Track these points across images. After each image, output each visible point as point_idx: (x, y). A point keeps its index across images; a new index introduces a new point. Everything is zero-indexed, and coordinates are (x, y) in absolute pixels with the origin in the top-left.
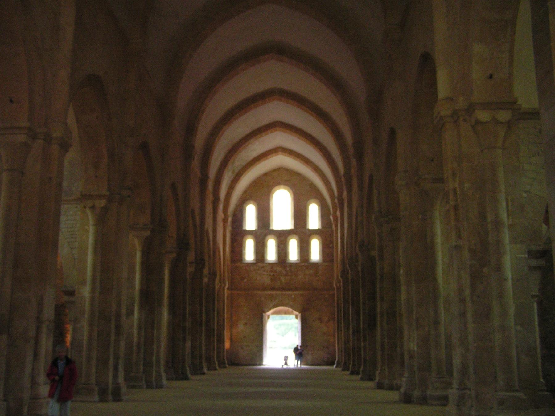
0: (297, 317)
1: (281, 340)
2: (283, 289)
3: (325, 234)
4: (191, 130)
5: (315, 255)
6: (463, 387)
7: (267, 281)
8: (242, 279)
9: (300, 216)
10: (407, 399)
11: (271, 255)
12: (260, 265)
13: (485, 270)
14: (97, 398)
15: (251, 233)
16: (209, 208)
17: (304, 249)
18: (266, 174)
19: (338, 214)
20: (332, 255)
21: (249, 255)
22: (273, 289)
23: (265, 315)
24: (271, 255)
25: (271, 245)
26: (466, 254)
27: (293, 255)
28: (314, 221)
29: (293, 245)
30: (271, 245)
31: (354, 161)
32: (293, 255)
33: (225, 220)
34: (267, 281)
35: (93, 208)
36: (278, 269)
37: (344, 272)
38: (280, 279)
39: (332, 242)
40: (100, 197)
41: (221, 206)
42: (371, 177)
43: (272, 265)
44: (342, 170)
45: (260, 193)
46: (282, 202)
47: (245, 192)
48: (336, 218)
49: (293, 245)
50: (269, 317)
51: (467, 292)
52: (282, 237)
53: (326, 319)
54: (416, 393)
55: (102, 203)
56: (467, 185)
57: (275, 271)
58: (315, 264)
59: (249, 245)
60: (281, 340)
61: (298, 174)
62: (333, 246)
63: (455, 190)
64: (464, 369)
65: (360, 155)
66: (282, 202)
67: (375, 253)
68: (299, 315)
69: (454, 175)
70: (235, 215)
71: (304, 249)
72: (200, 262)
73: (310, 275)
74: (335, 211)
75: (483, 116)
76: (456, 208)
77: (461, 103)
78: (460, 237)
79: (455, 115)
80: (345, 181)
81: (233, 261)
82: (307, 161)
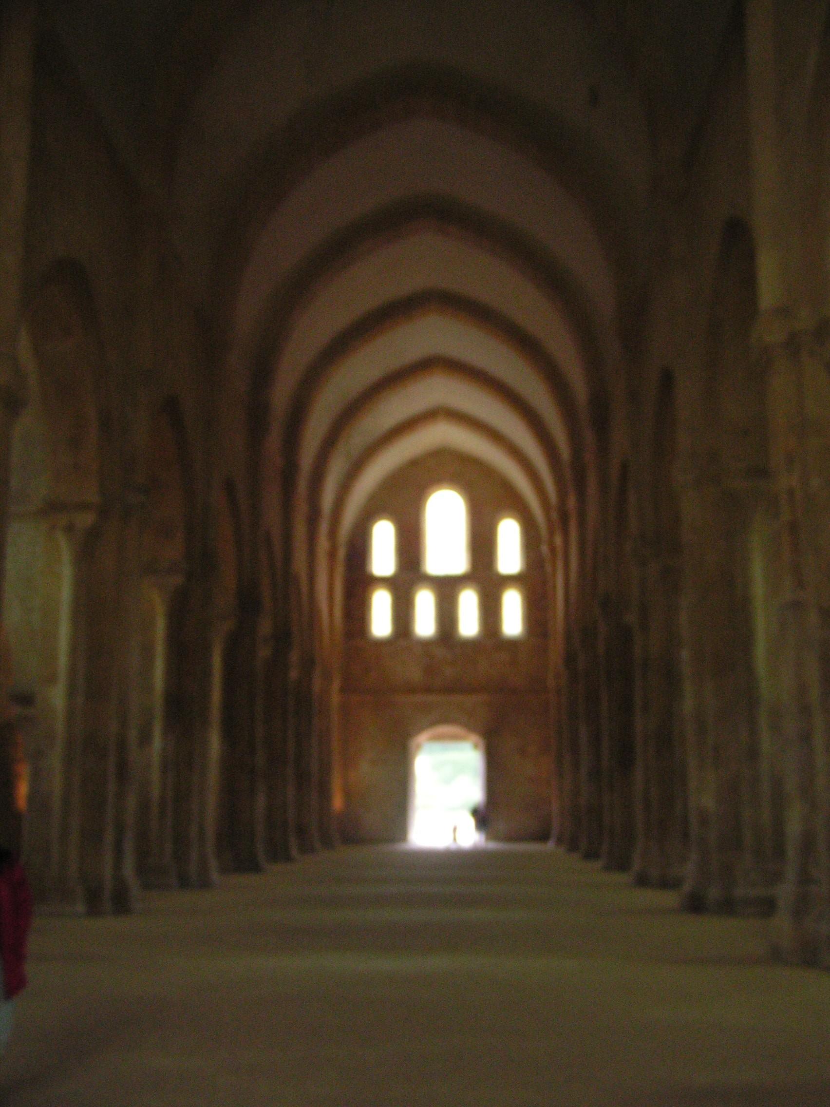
1: (445, 795)
3: (533, 582)
4: (263, 372)
6: (805, 879)
7: (414, 673)
9: (482, 545)
10: (696, 905)
11: (425, 624)
14: (81, 907)
16: (300, 530)
17: (490, 611)
18: (414, 463)
19: (558, 540)
21: (381, 621)
22: (428, 690)
24: (425, 624)
25: (425, 603)
26: (813, 617)
27: (469, 624)
29: (468, 603)
30: (425, 603)
31: (589, 437)
32: (469, 624)
33: (332, 555)
34: (414, 673)
35: (69, 529)
37: (570, 659)
40: (83, 507)
41: (324, 528)
42: (624, 468)
43: (426, 644)
46: (446, 516)
48: (553, 549)
49: (468, 603)
50: (418, 747)
54: (714, 893)
56: (815, 482)
58: (512, 644)
60: (445, 795)
63: (791, 492)
64: (808, 845)
65: (601, 422)
66: (446, 516)
67: (631, 618)
71: (490, 611)
72: (282, 638)
74: (551, 534)
76: (793, 527)
80: (572, 475)
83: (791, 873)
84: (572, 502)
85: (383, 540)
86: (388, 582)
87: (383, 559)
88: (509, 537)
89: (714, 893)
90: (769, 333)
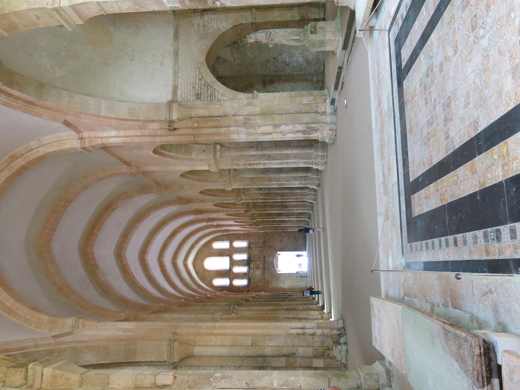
0: (279, 254)
2: (264, 263)
3: (232, 237)
5: (243, 244)
6: (312, 163)
7: (258, 272)
8: (258, 286)
9: (221, 253)
11: (244, 269)
12: (250, 275)
13: (272, 155)
17: (240, 251)
18: (197, 273)
20: (244, 235)
21: (244, 282)
23: (279, 272)
24: (244, 269)
25: (237, 270)
27: (244, 257)
28: (224, 245)
29: (237, 257)
30: (237, 270)
34: (258, 272)
36: (252, 265)
38: (258, 264)
39: (237, 234)
44: (204, 224)
45: (207, 276)
47: (207, 285)
49: (237, 257)
51: (280, 161)
52: (233, 263)
53: (280, 238)
57: (254, 267)
59: (238, 282)
61: (197, 254)
62: (240, 234)
63: (243, 165)
64: (306, 163)
68: (278, 253)
69: (238, 165)
71: (240, 251)
73: (255, 247)
75: (218, 154)
77: (212, 161)
78: (260, 164)
81: (248, 291)
83: (311, 166)
84: (215, 223)
85: (219, 282)
87: (225, 282)
88: (218, 245)
89: (316, 182)
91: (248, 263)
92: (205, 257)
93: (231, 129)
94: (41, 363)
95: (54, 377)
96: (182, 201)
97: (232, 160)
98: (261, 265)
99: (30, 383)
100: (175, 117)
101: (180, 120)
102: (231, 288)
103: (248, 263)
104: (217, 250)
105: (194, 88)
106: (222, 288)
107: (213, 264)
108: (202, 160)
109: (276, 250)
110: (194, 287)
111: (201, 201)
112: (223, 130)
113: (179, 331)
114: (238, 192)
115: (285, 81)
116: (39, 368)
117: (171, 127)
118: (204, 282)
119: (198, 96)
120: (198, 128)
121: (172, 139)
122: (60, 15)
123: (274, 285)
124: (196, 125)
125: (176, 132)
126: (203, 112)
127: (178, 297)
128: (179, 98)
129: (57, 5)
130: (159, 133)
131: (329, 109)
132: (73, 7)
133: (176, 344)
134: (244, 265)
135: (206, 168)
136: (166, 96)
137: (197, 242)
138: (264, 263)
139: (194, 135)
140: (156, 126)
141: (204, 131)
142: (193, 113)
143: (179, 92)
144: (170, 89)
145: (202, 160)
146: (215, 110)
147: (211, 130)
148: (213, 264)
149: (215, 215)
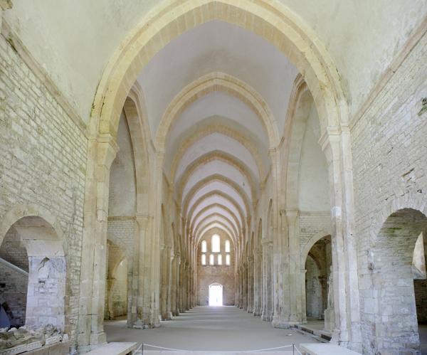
1: (215, 296)
2: (216, 276)
3: (232, 254)
4: (188, 225)
5: (228, 262)
7: (209, 271)
9: (222, 247)
10: (255, 315)
11: (212, 262)
15: (204, 253)
17: (224, 259)
21: (204, 262)
24: (212, 262)
25: (212, 257)
27: (220, 263)
28: (228, 249)
29: (220, 257)
30: (212, 257)
36: (214, 268)
37: (238, 272)
45: (208, 238)
49: (220, 257)
52: (216, 255)
55: (172, 258)
58: (228, 266)
59: (204, 257)
60: (215, 296)
61: (222, 230)
70: (198, 247)
71: (224, 259)
72: (190, 268)
77: (267, 241)
79: (265, 244)
81: (198, 265)
82: (226, 226)
85: (204, 245)
86: (220, 275)
87: (204, 249)
88: (227, 244)
90: (262, 242)
91: (216, 265)
92: (220, 235)
93: (281, 254)
94: (112, 141)
95: (104, 150)
96: (249, 218)
97: (268, 255)
98: (214, 274)
99: (101, 136)
100: (287, 214)
101: (286, 217)
102: (199, 253)
103: (216, 265)
104: (225, 243)
105: (309, 227)
106: (200, 248)
107: (216, 240)
108: (268, 233)
109: (224, 284)
110: (200, 228)
111: (249, 232)
112: (280, 248)
113: (154, 220)
114: (252, 258)
115: (323, 293)
116: (108, 140)
117: (282, 212)
118: (204, 235)
119: (303, 230)
120: (282, 231)
121: (275, 212)
122: (324, 136)
123: (202, 283)
124: (283, 229)
125: (279, 215)
126: (292, 233)
127: (190, 218)
128: (301, 217)
129: (329, 133)
130: (279, 204)
131: (292, 323)
132: (329, 145)
133: (146, 219)
134: (214, 262)
135: (263, 237)
136: (303, 207)
137: (229, 230)
138: (216, 276)
139: (277, 228)
140: (283, 201)
141: (279, 235)
142: (290, 227)
143: (306, 217)
144: (309, 210)
145: (268, 233)
146: (294, 243)
147: (280, 241)
148: (216, 240)
149: (243, 242)
